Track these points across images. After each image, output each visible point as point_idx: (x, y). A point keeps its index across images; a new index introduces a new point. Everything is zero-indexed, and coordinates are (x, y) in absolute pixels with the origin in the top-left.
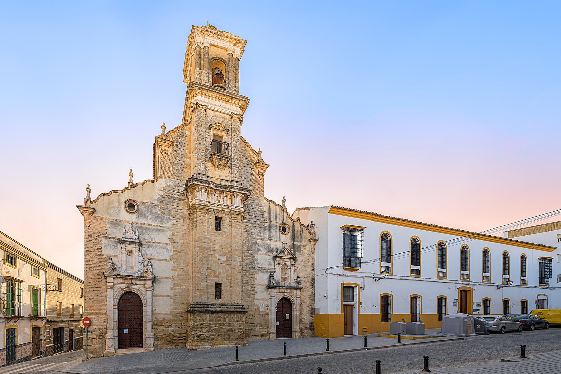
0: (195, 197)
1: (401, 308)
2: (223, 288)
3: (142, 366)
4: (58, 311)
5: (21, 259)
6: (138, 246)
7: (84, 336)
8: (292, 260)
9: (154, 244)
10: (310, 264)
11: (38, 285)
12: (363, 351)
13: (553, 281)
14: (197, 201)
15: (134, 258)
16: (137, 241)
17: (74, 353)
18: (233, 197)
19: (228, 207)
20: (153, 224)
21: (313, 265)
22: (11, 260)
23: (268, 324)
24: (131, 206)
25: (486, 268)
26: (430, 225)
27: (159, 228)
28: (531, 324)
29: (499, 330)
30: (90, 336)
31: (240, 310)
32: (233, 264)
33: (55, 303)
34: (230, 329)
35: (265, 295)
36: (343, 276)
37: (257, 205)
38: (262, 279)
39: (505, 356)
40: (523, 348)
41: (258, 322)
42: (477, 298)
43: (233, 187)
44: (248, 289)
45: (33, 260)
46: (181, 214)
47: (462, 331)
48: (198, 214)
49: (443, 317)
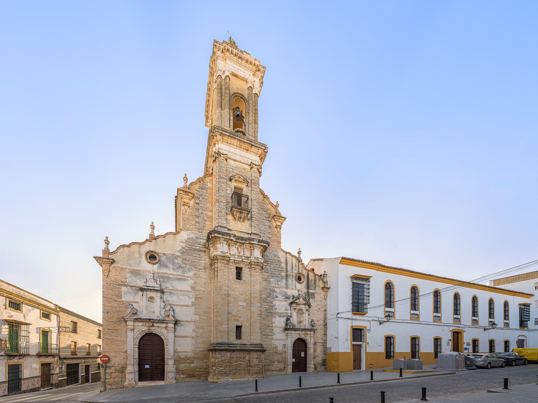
1: (402, 347)
3: (163, 396)
4: (73, 350)
5: (27, 305)
6: (159, 294)
7: (102, 371)
8: (307, 306)
9: (176, 292)
10: (323, 309)
11: (49, 328)
12: (370, 383)
13: (531, 324)
14: (218, 253)
15: (155, 303)
17: (91, 385)
18: (252, 248)
21: (325, 310)
22: (16, 306)
23: (285, 361)
25: (475, 313)
26: (427, 275)
27: (181, 277)
28: (513, 360)
29: (485, 366)
30: (108, 371)
31: (259, 348)
32: (253, 309)
33: (69, 343)
34: (250, 364)
35: (283, 336)
36: (352, 319)
37: (275, 256)
38: (279, 322)
39: (490, 388)
40: (506, 381)
41: (276, 359)
42: (467, 339)
43: (253, 239)
44: (267, 331)
45: (43, 305)
47: (454, 366)
49: (439, 355)
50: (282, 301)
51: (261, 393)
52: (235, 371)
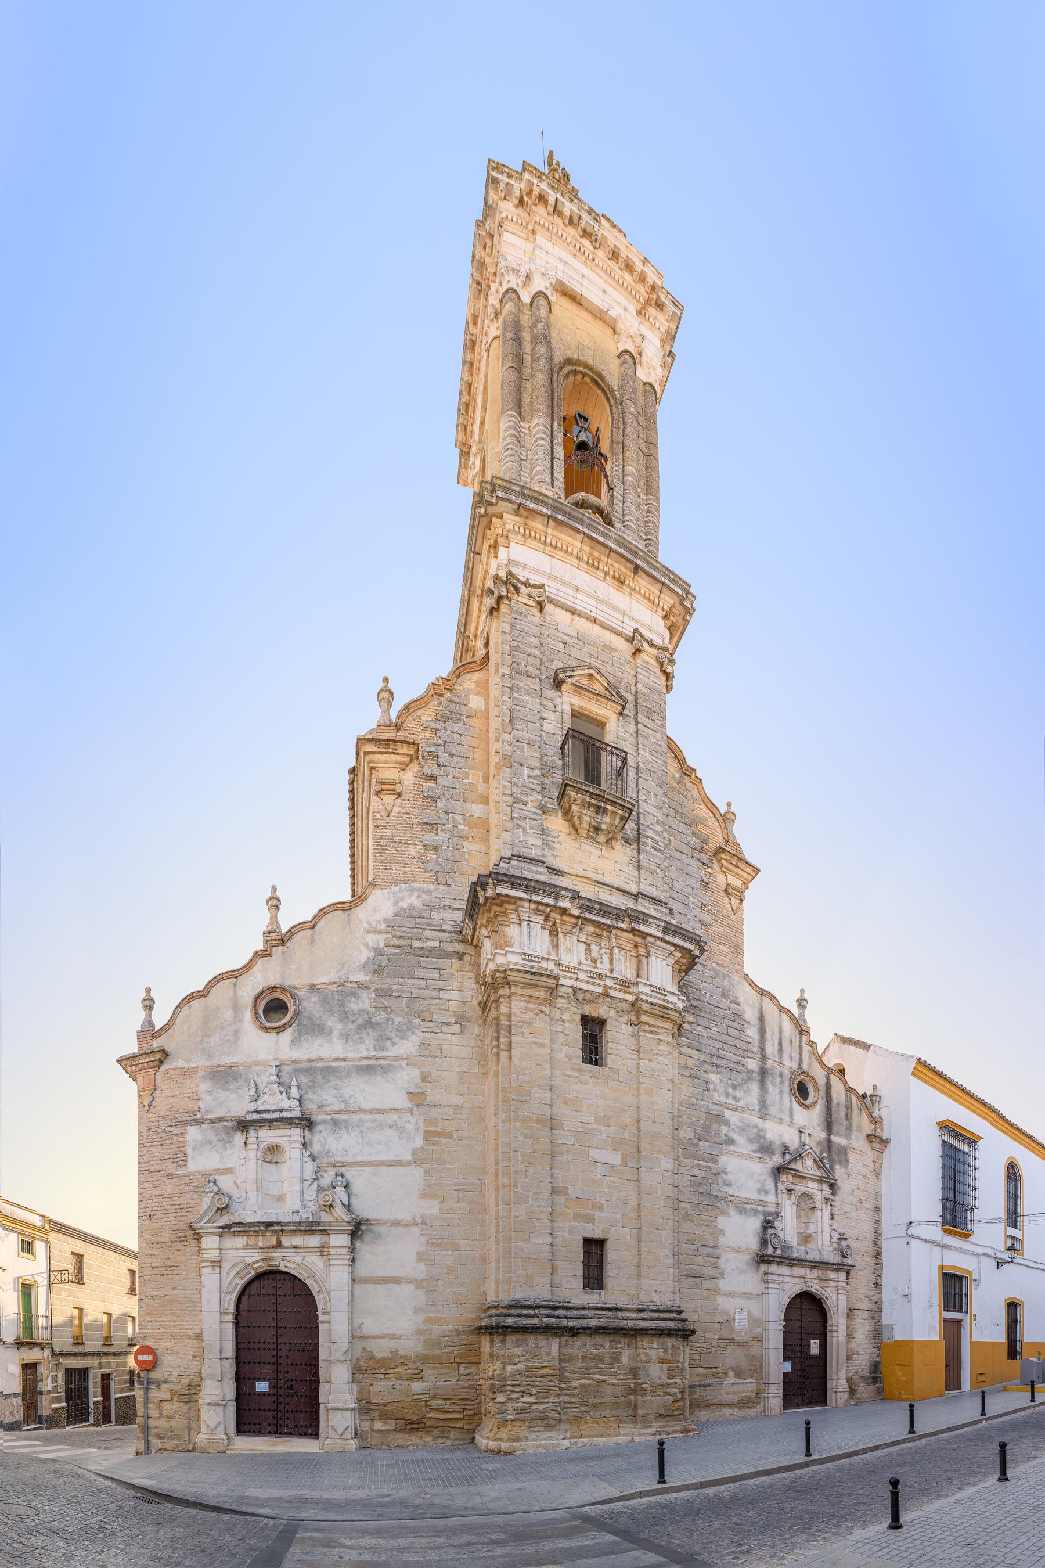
0: (503, 944)
2: (611, 1254)
9: (354, 1117)
16: (296, 1114)
19: (626, 985)
20: (351, 1055)
23: (757, 1369)
24: (274, 1007)
27: (374, 1062)
31: (671, 1325)
38: (740, 1232)
41: (730, 1362)
43: (643, 918)
44: (697, 1264)
46: (453, 1006)
48: (518, 1006)
50: (747, 1157)
51: (679, 1489)
52: (579, 1408)
